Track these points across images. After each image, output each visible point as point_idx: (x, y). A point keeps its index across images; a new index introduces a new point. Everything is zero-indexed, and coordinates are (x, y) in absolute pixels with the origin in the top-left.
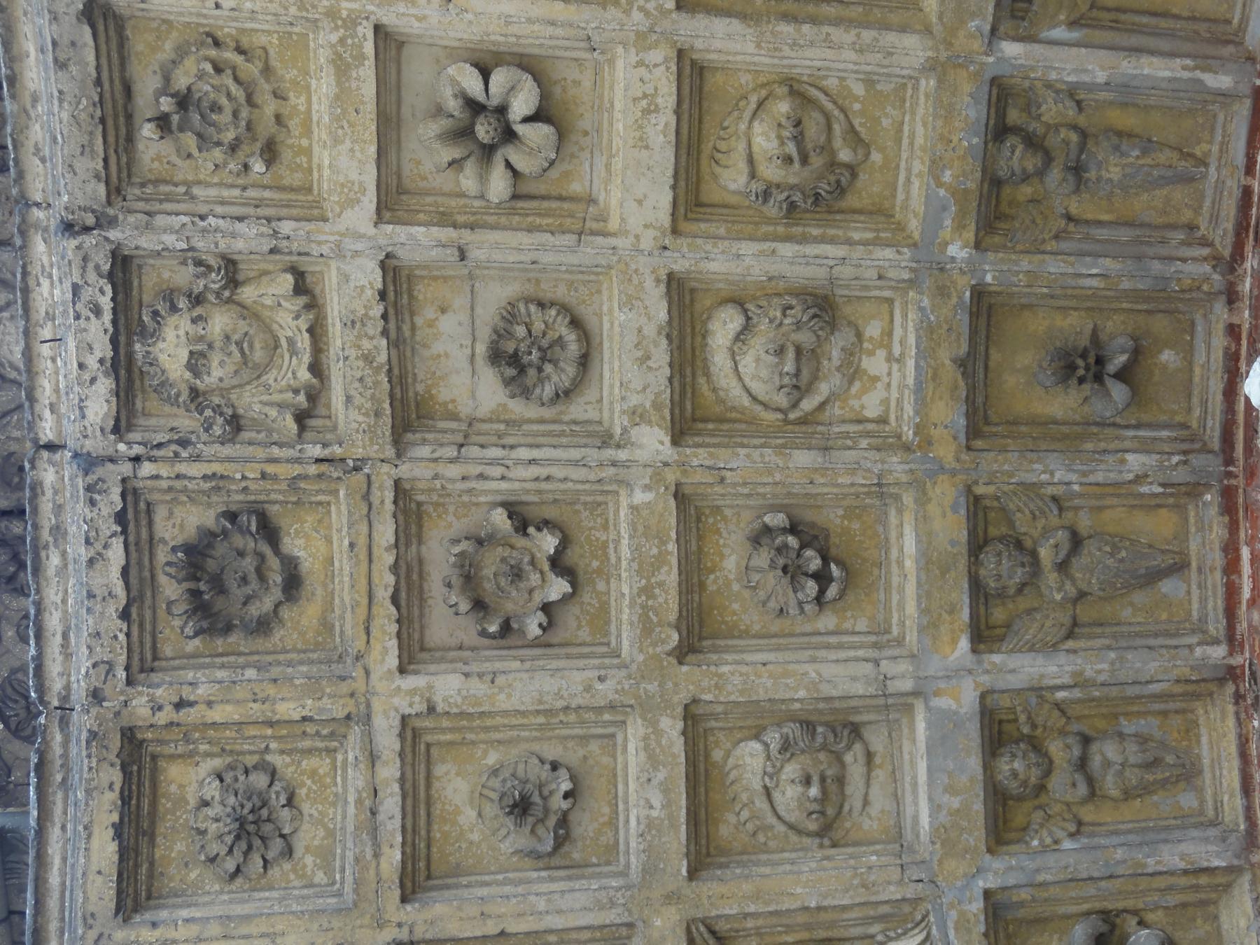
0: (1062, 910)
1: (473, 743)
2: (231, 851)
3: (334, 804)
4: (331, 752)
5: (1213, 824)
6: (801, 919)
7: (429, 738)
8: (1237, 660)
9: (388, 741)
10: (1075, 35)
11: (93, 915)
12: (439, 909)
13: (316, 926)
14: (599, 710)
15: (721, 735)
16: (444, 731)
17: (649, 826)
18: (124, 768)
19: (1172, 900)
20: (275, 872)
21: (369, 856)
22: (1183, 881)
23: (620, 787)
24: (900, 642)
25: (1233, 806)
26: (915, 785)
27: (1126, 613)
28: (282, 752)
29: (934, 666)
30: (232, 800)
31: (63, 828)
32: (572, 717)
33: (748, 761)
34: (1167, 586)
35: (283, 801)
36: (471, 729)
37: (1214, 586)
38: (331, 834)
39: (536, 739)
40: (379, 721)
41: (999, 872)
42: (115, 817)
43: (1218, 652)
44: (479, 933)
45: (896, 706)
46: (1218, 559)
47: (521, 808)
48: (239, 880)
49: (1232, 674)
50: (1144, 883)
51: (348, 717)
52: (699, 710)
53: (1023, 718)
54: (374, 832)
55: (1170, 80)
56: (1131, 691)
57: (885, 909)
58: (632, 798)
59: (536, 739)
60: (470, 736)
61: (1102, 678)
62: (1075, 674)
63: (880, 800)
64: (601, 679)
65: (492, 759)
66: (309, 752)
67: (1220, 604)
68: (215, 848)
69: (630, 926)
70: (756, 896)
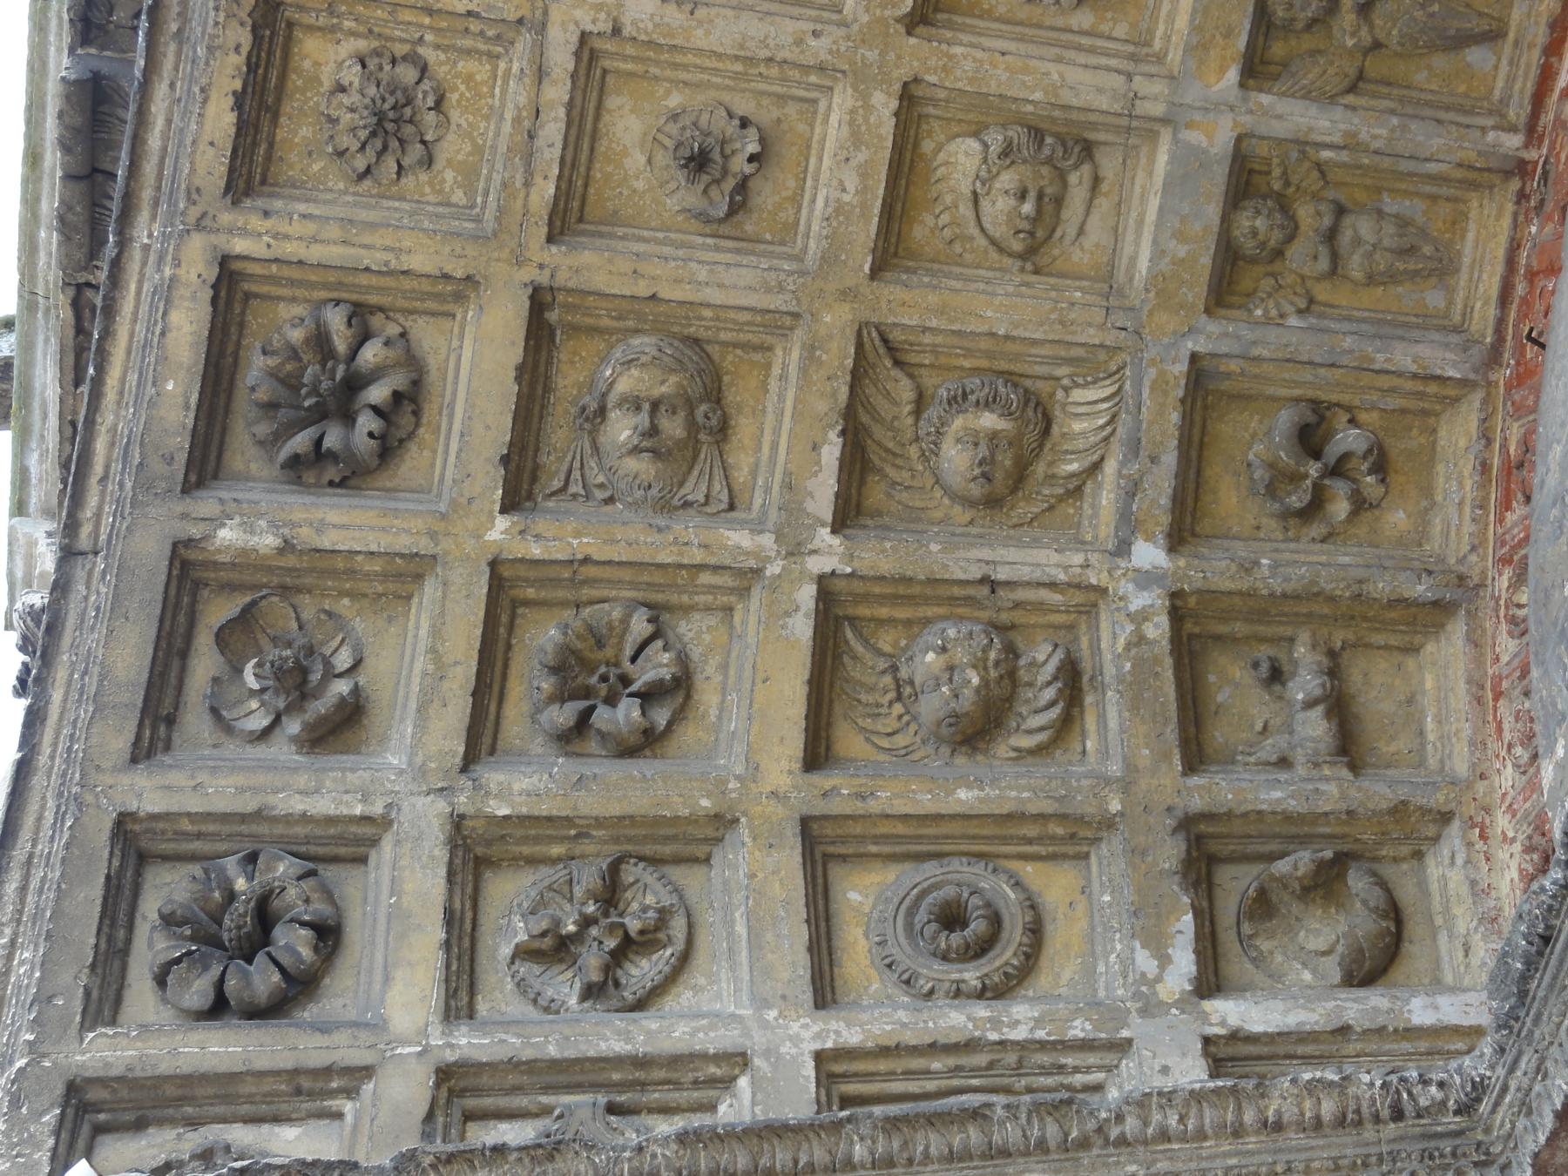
0: (1270, 391)
1: (656, 78)
2: (363, 147)
3: (487, 118)
4: (493, 57)
5: (1457, 330)
6: (984, 344)
7: (607, 63)
8: (1531, 155)
9: (561, 59)
11: (198, 190)
12: (587, 257)
13: (447, 249)
14: (806, 69)
15: (936, 124)
16: (625, 58)
17: (837, 210)
18: (255, 29)
19: (1393, 403)
20: (408, 181)
21: (518, 184)
22: (1409, 385)
23: (813, 161)
24: (1160, 58)
25: (1484, 316)
26: (1140, 223)
27: (1420, 77)
28: (437, 47)
29: (1192, 94)
30: (372, 91)
31: (172, 85)
32: (774, 71)
33: (959, 159)
34: (1476, 56)
35: (430, 102)
36: (657, 63)
37: (1528, 66)
38: (478, 150)
39: (728, 88)
40: (554, 32)
41: (1213, 336)
42: (238, 85)
43: (1512, 142)
44: (628, 293)
45: (1138, 129)
47: (698, 163)
48: (367, 183)
49: (1522, 168)
50: (1366, 379)
51: (520, 21)
52: (919, 91)
53: (1277, 172)
54: (529, 158)
56: (1406, 166)
57: (1080, 352)
58: (825, 175)
59: (728, 88)
60: (654, 70)
61: (1376, 145)
62: (1347, 134)
63: (1097, 231)
64: (816, 34)
65: (675, 101)
66: (468, 52)
67: (1530, 87)
68: (346, 141)
69: (796, 316)
70: (941, 311)
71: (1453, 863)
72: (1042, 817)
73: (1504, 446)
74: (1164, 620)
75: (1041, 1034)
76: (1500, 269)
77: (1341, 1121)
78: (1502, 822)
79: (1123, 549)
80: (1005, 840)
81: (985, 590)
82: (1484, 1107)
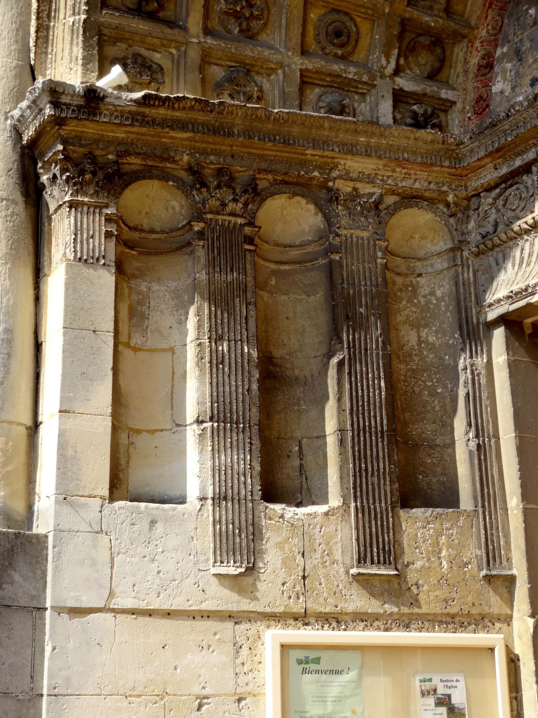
71: (462, 50)
75: (356, 77)
77: (432, 142)
78: (477, 44)
82: (461, 146)
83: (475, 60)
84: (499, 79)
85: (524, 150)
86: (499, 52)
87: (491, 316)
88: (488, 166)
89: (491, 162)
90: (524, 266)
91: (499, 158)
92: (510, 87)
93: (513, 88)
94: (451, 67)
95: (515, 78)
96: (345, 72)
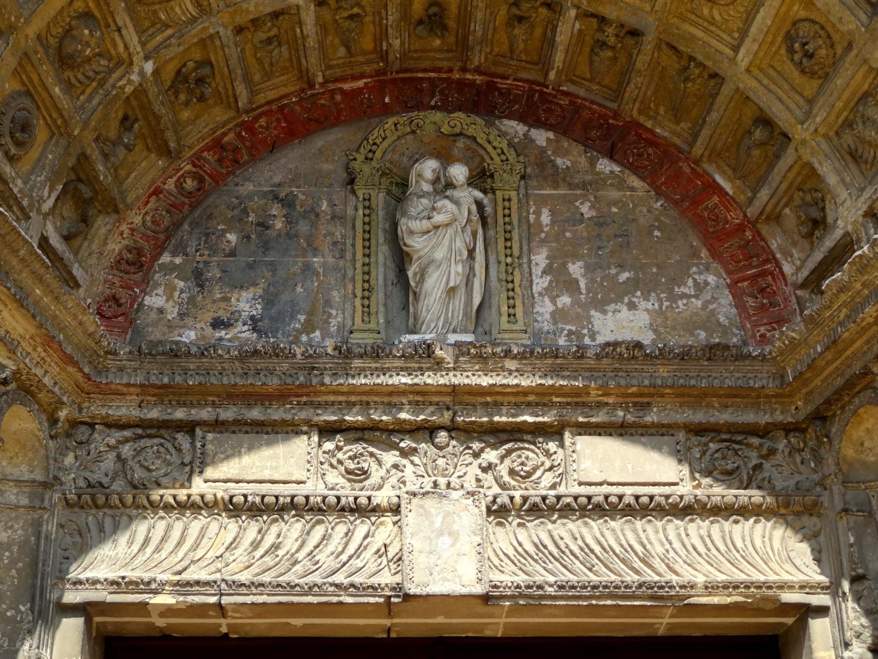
10: (576, 31)
19: (221, 90)
22: (230, 93)
25: (261, 99)
27: (330, 38)
37: (344, 71)
46: (357, 70)
49: (311, 86)
50: (228, 81)
55: (554, 61)
56: (302, 53)
61: (307, 45)
62: (308, 36)
71: (105, 225)
72: (62, 116)
73: (224, 134)
74: (132, 88)
76: (277, 96)
78: (124, 227)
79: (147, 58)
80: (47, 109)
81: (115, 29)
82: (109, 356)
83: (115, 246)
84: (160, 291)
85: (195, 402)
86: (165, 258)
87: (71, 597)
88: (129, 397)
89: (137, 395)
90: (149, 550)
91: (154, 395)
92: (176, 310)
93: (182, 315)
94: (85, 238)
95: (187, 303)
96: (13, 182)
